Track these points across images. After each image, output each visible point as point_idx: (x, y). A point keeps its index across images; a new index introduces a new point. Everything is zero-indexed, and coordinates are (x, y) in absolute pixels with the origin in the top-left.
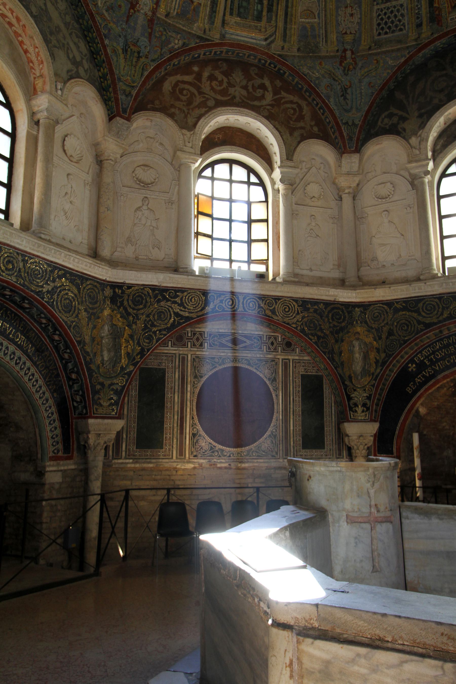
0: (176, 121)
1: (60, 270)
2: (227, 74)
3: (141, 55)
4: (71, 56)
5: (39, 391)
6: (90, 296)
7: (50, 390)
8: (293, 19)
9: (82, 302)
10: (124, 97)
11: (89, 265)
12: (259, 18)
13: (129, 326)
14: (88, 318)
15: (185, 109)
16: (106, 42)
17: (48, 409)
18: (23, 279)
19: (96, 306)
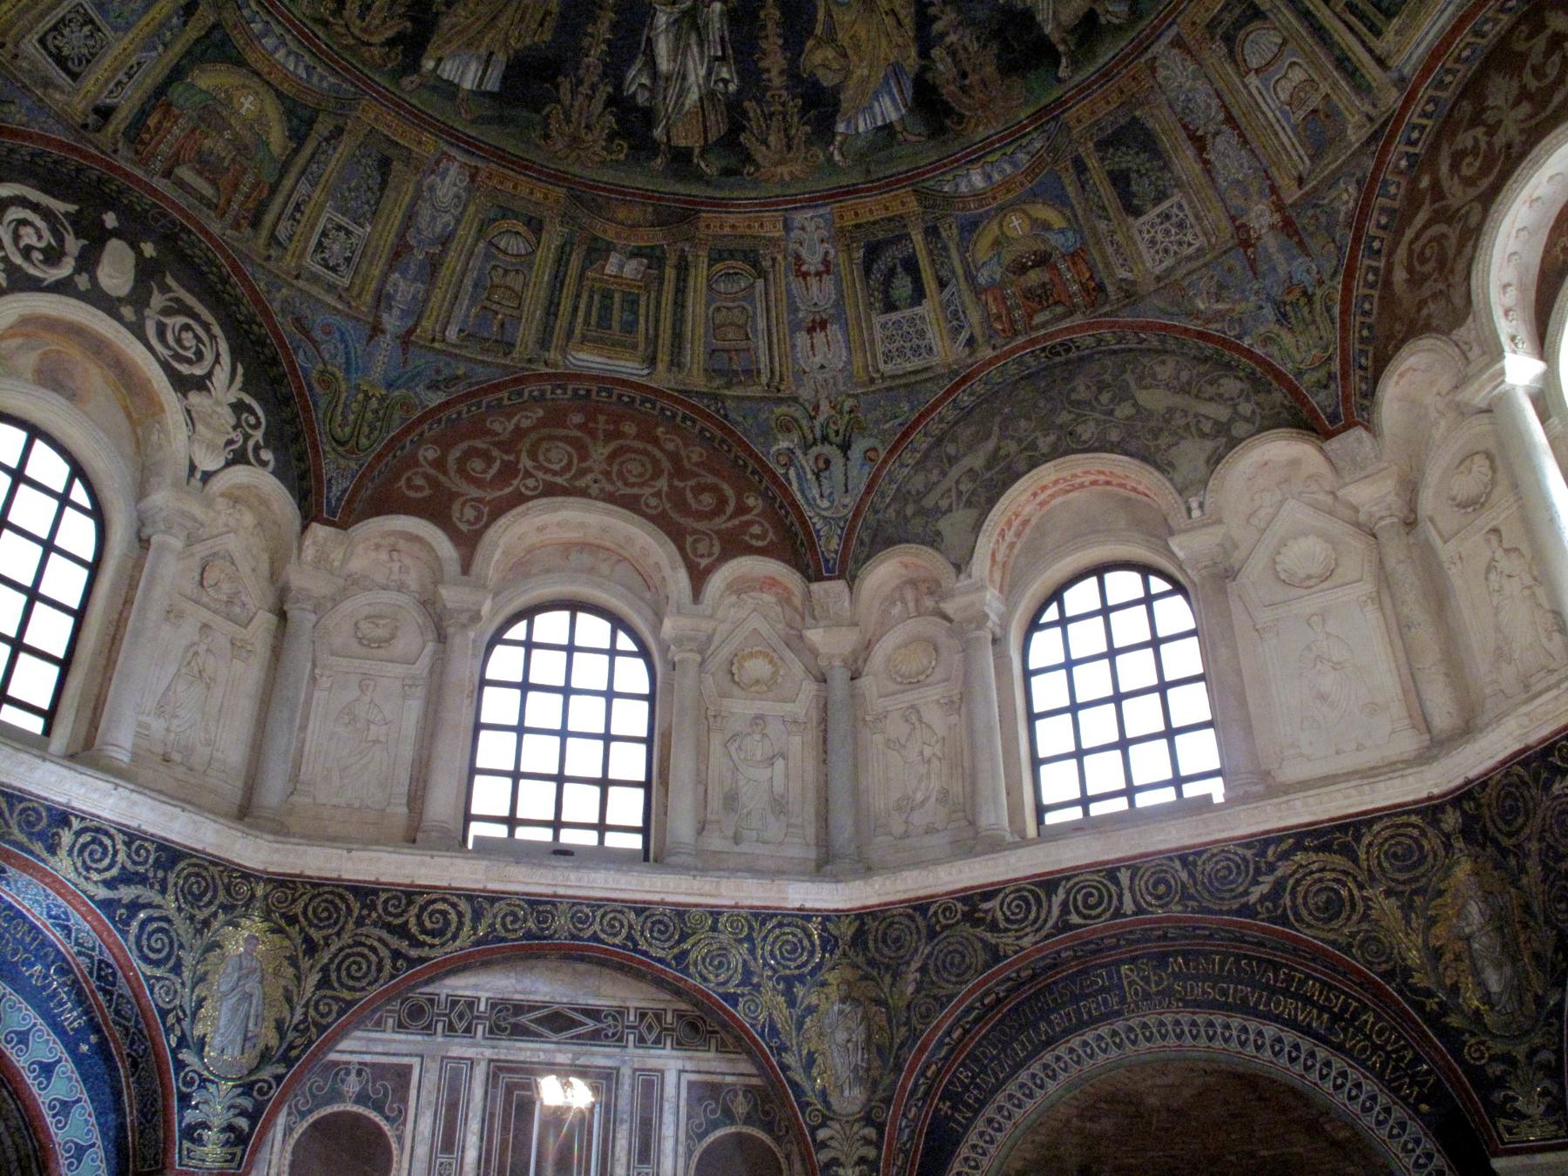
0: (1437, 330)
1: (1280, 840)
2: (1475, 121)
3: (1310, 290)
4: (1207, 430)
5: (1371, 1109)
6: (1395, 855)
7: (1404, 1099)
9: (1372, 878)
10: (1322, 394)
11: (1353, 792)
13: (1515, 882)
14: (1401, 908)
15: (1441, 286)
16: (1246, 342)
17: (1410, 1146)
18: (1194, 899)
19: (1422, 870)
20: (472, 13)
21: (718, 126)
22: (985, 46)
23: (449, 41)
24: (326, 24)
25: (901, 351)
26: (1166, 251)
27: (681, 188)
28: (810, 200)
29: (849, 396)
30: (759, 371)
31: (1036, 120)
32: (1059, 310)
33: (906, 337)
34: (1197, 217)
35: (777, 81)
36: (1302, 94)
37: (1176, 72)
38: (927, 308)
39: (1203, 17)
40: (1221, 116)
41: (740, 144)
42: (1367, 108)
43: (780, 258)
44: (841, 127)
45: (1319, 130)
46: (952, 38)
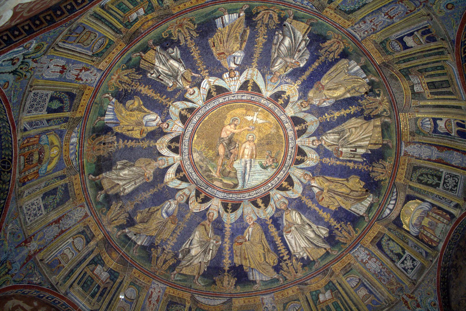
8: (113, 308)
12: (93, 296)
20: (236, 32)
21: (143, 65)
22: (108, 153)
23: (239, 22)
24: (282, 10)
25: (35, 100)
26: (29, 210)
27: (138, 44)
28: (101, 81)
29: (31, 76)
30: (64, 42)
31: (81, 165)
32: (22, 167)
33: (39, 103)
34: (36, 221)
35: (140, 88)
36: (65, 258)
37: (78, 214)
38: (44, 115)
39: (90, 224)
40: (63, 229)
41: (133, 68)
42: (60, 282)
43: (93, 64)
44: (114, 100)
45: (55, 266)
46: (115, 145)
